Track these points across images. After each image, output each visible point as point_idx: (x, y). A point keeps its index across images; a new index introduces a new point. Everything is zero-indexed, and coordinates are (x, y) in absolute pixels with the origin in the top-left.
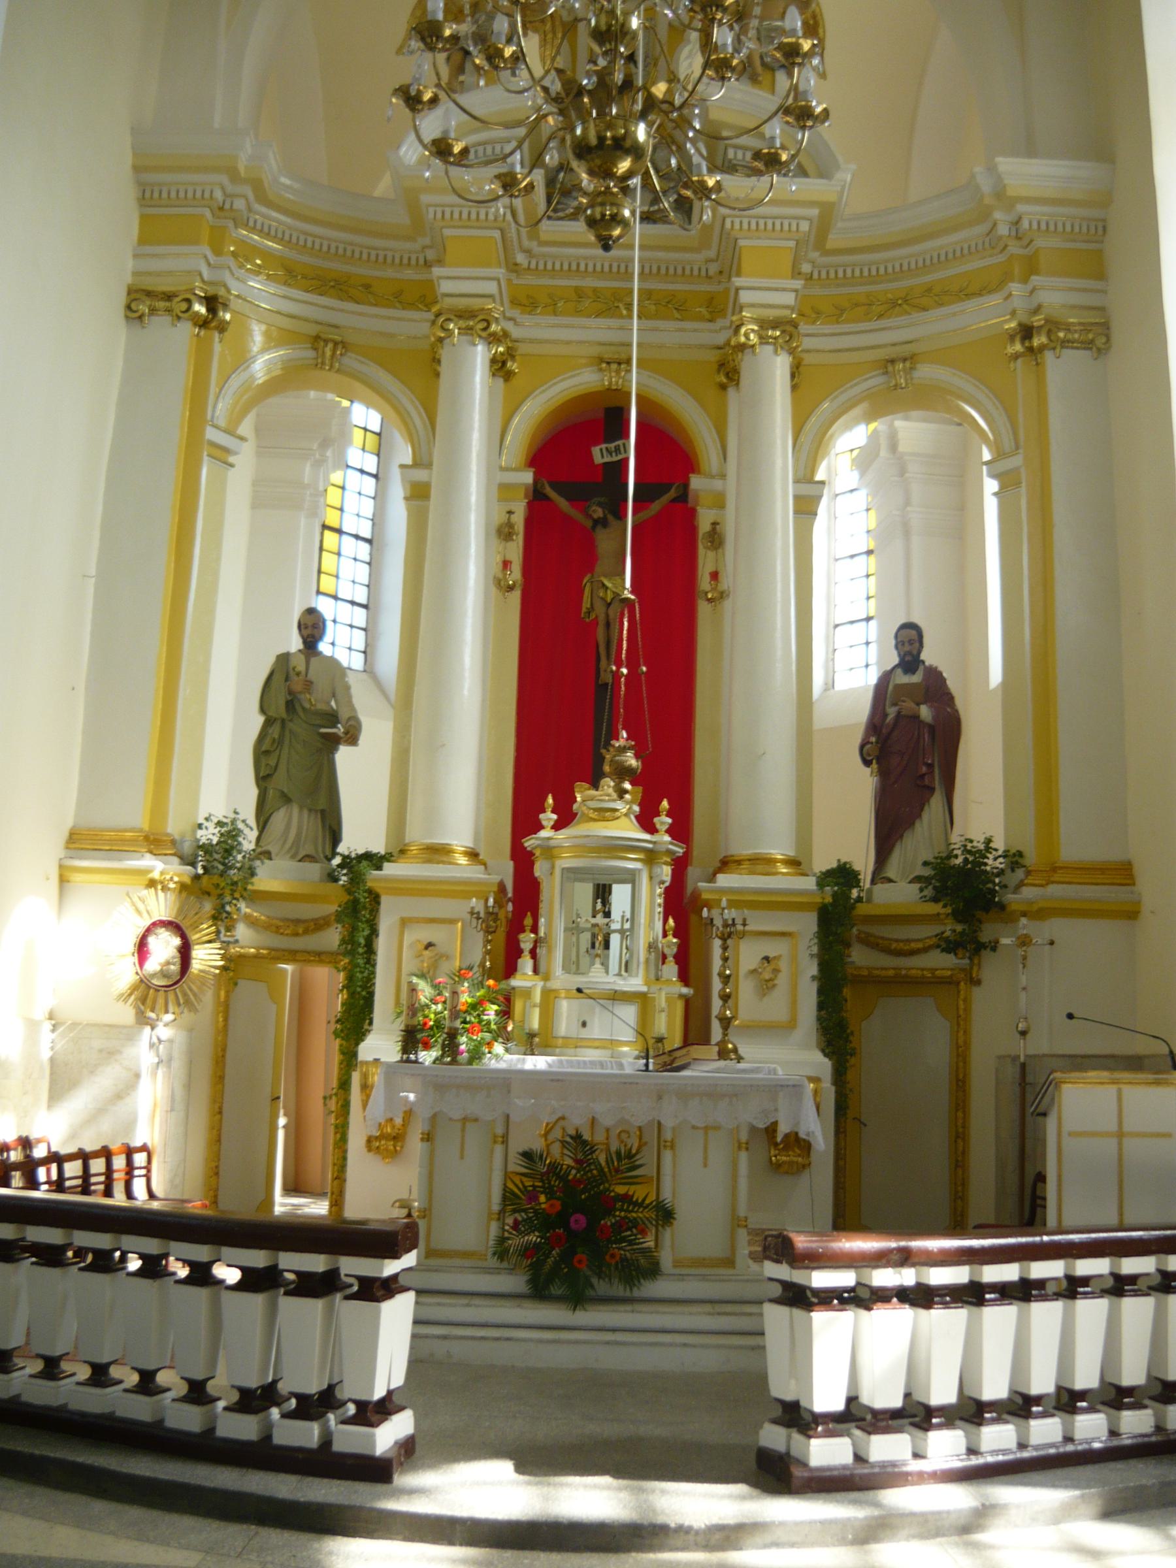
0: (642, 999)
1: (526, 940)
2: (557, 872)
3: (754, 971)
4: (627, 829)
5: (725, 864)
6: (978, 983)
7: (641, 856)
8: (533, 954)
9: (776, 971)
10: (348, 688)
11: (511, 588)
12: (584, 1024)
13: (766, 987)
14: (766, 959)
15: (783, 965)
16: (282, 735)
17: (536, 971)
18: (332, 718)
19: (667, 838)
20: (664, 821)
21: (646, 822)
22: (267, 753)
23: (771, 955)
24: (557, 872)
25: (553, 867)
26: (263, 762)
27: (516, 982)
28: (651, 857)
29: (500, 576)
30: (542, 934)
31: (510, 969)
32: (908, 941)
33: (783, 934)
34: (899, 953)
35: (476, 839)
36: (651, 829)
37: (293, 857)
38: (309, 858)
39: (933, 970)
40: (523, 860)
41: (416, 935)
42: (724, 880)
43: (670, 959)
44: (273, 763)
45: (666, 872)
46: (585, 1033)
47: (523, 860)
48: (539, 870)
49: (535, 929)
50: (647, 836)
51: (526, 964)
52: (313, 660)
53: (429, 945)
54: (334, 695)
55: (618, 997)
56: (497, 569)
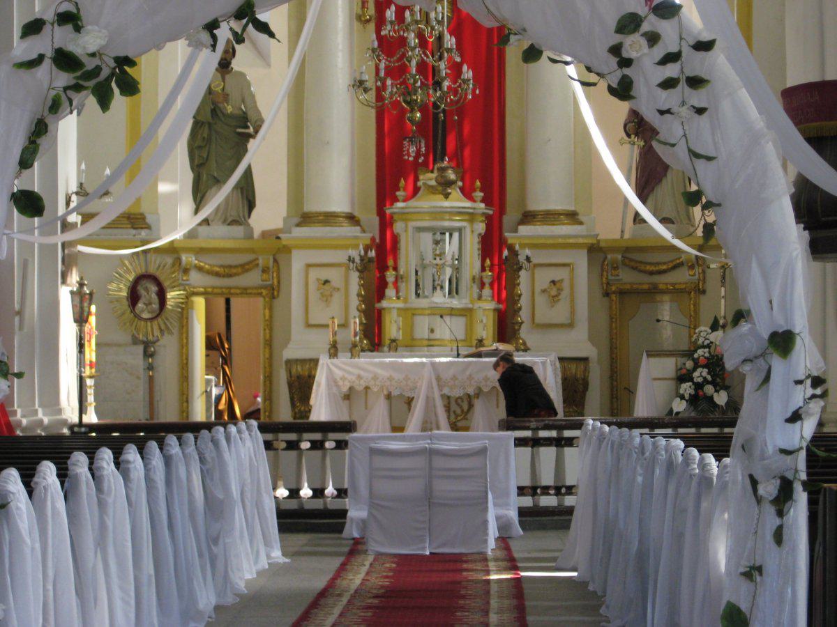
0: (466, 313)
1: (390, 276)
2: (410, 230)
3: (544, 291)
4: (457, 201)
5: (528, 217)
6: (704, 292)
7: (467, 217)
8: (396, 284)
9: (560, 290)
10: (253, 96)
11: (368, 21)
12: (432, 331)
13: (555, 299)
14: (553, 282)
15: (566, 285)
16: (210, 135)
17: (398, 298)
18: (243, 120)
19: (482, 205)
20: (479, 195)
21: (467, 193)
22: (200, 147)
23: (556, 279)
24: (410, 230)
25: (406, 226)
26: (197, 152)
27: (384, 304)
28: (471, 217)
29: (360, 12)
30: (402, 271)
31: (381, 295)
32: (658, 264)
33: (564, 265)
34: (651, 273)
35: (352, 203)
36: (471, 199)
37: (224, 222)
38: (235, 222)
39: (673, 284)
40: (386, 222)
41: (315, 274)
42: (524, 230)
43: (487, 286)
44: (205, 156)
45: (481, 227)
46: (432, 336)
47: (386, 222)
48: (398, 227)
49: (395, 269)
50: (468, 204)
51: (390, 292)
52: (228, 77)
53: (326, 282)
54: (243, 101)
55: (452, 312)
56: (357, 9)
